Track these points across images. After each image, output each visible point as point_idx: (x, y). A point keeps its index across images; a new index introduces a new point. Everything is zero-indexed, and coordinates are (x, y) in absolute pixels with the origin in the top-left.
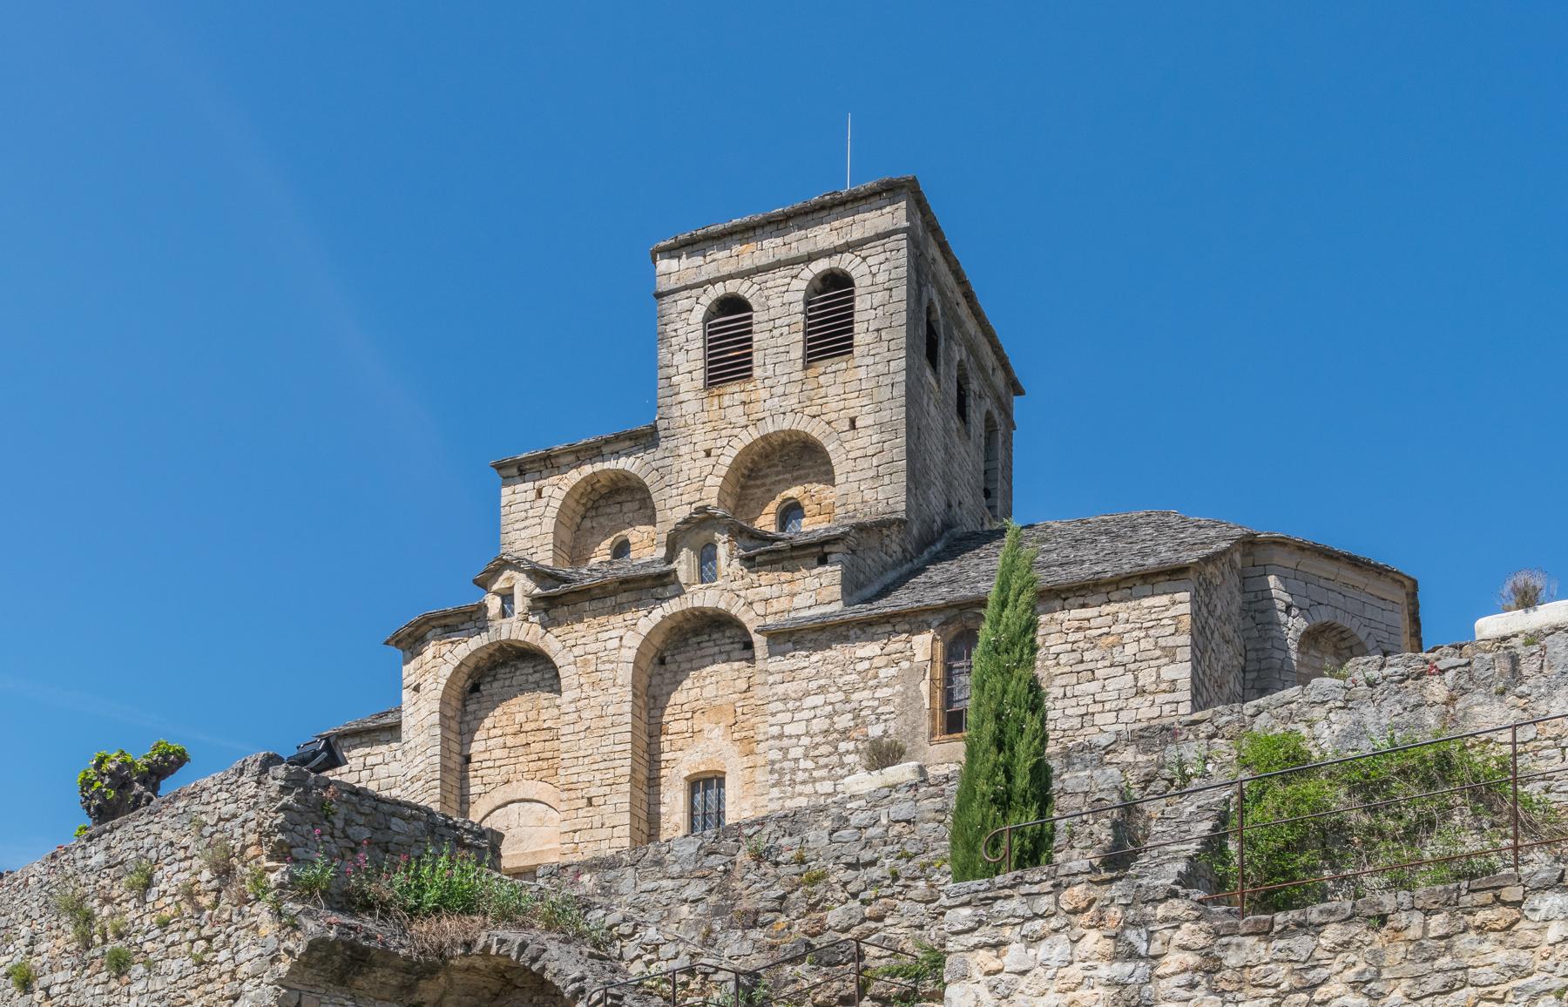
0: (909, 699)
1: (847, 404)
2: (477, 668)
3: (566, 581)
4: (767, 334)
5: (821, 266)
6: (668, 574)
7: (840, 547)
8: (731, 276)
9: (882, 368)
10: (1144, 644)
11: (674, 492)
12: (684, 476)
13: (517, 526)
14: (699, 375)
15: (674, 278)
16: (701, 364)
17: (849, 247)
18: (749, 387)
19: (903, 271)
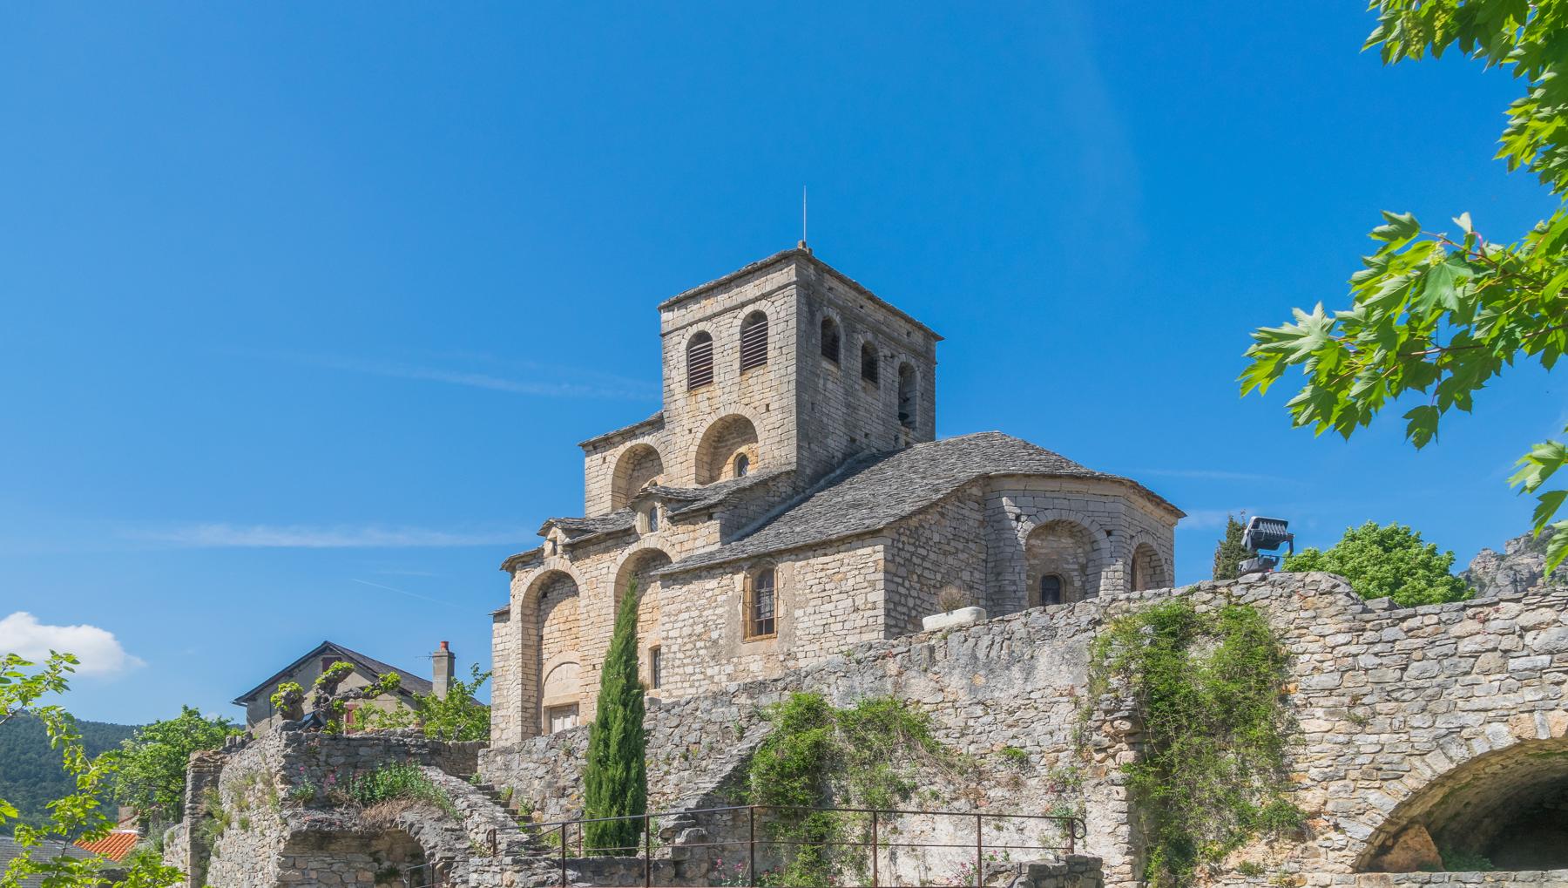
0: (732, 615)
1: (765, 395)
2: (543, 584)
3: (590, 531)
4: (720, 355)
5: (749, 309)
6: (629, 529)
7: (720, 508)
8: (700, 320)
9: (783, 372)
10: (859, 579)
11: (673, 456)
12: (678, 446)
13: (595, 480)
14: (685, 382)
15: (671, 323)
16: (685, 376)
17: (764, 296)
18: (711, 389)
19: (794, 309)
